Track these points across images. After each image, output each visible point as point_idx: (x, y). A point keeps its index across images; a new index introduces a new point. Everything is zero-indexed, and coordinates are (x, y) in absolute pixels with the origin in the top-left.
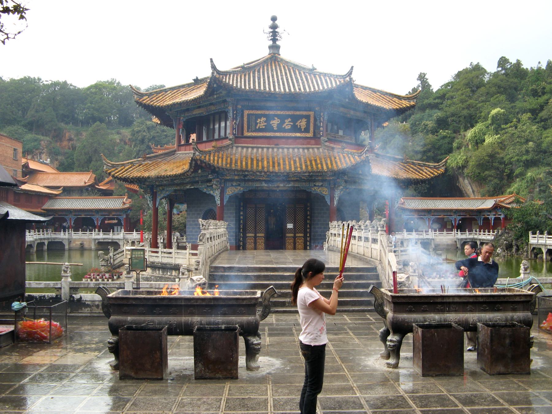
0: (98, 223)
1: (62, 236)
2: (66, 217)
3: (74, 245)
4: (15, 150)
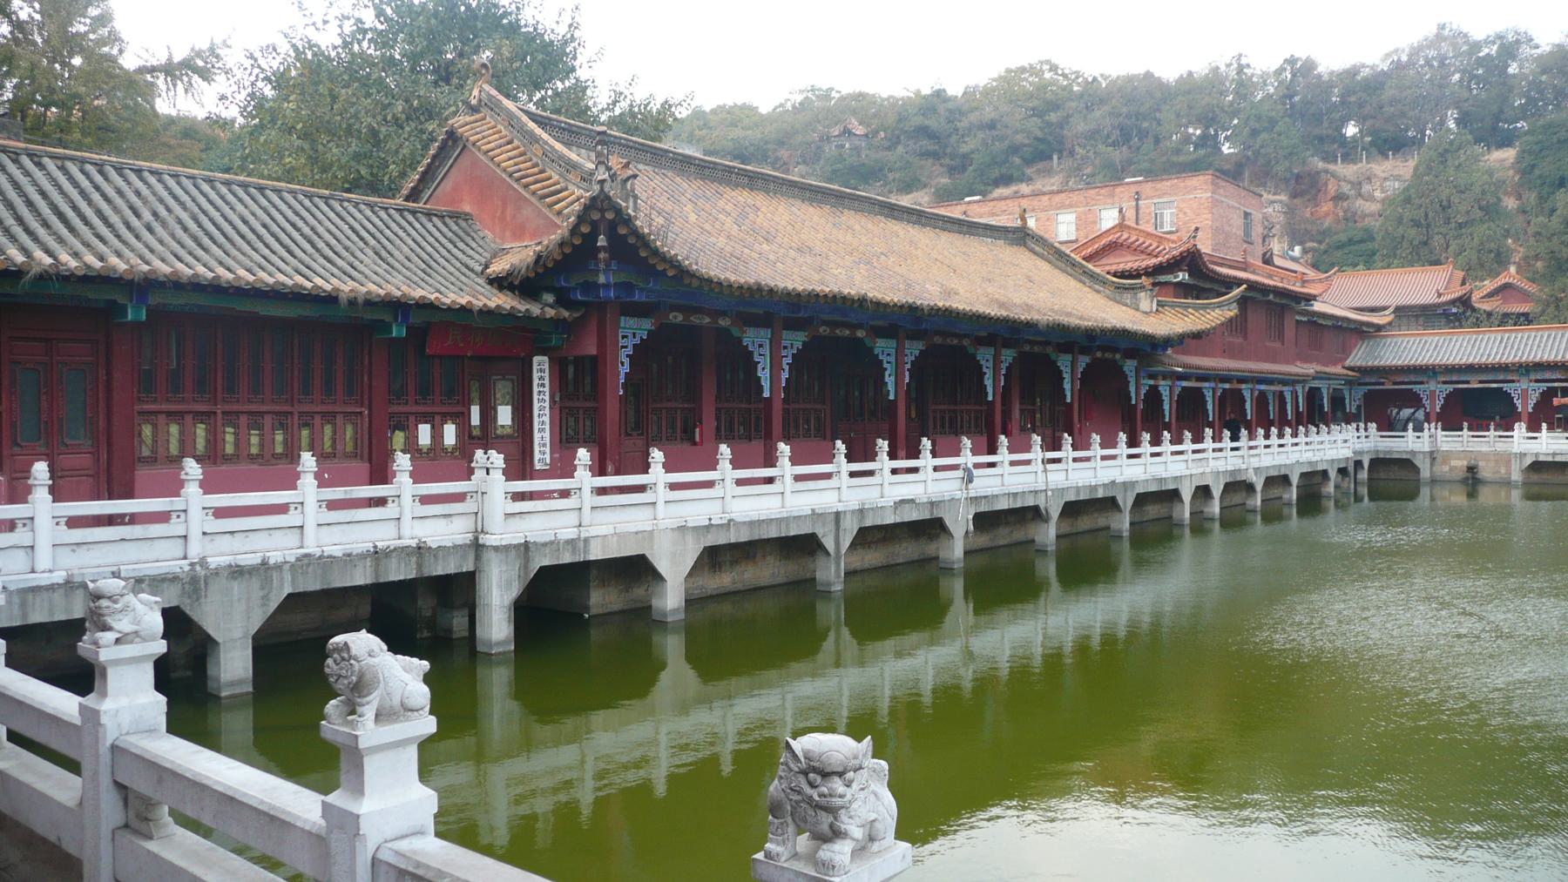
0: (1525, 404)
1: (1410, 442)
2: (1416, 388)
3: (1446, 468)
4: (1246, 215)
